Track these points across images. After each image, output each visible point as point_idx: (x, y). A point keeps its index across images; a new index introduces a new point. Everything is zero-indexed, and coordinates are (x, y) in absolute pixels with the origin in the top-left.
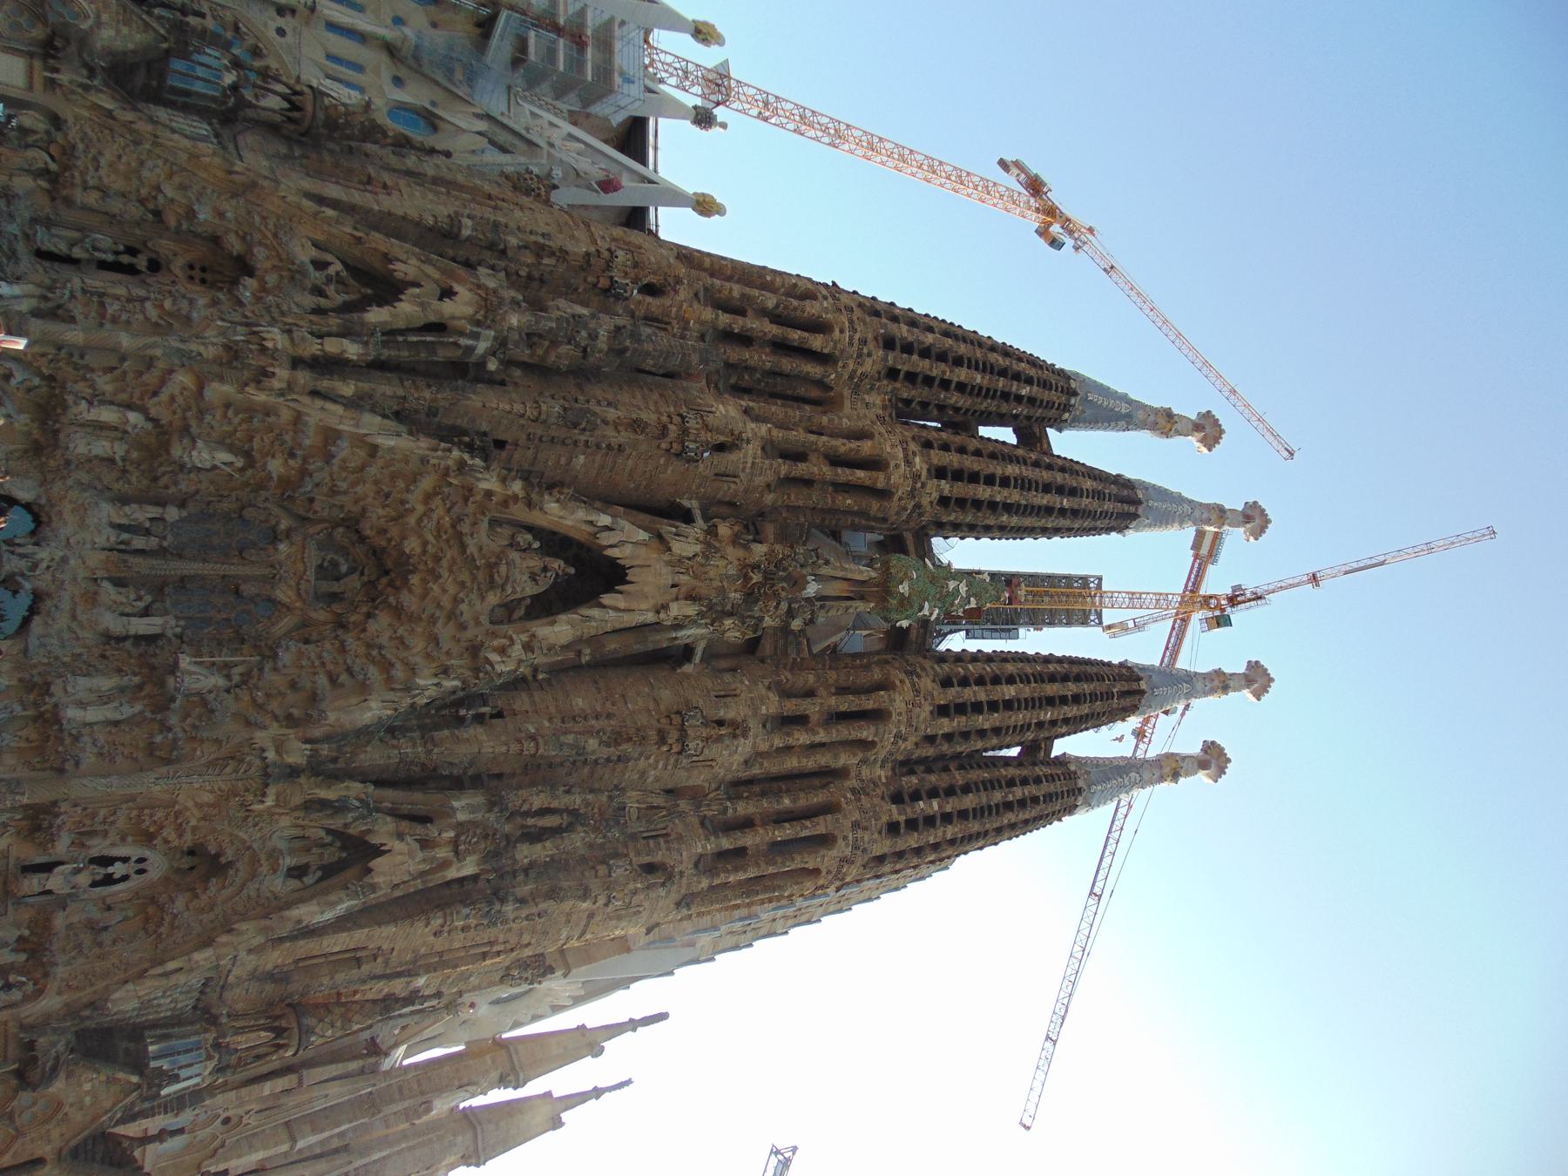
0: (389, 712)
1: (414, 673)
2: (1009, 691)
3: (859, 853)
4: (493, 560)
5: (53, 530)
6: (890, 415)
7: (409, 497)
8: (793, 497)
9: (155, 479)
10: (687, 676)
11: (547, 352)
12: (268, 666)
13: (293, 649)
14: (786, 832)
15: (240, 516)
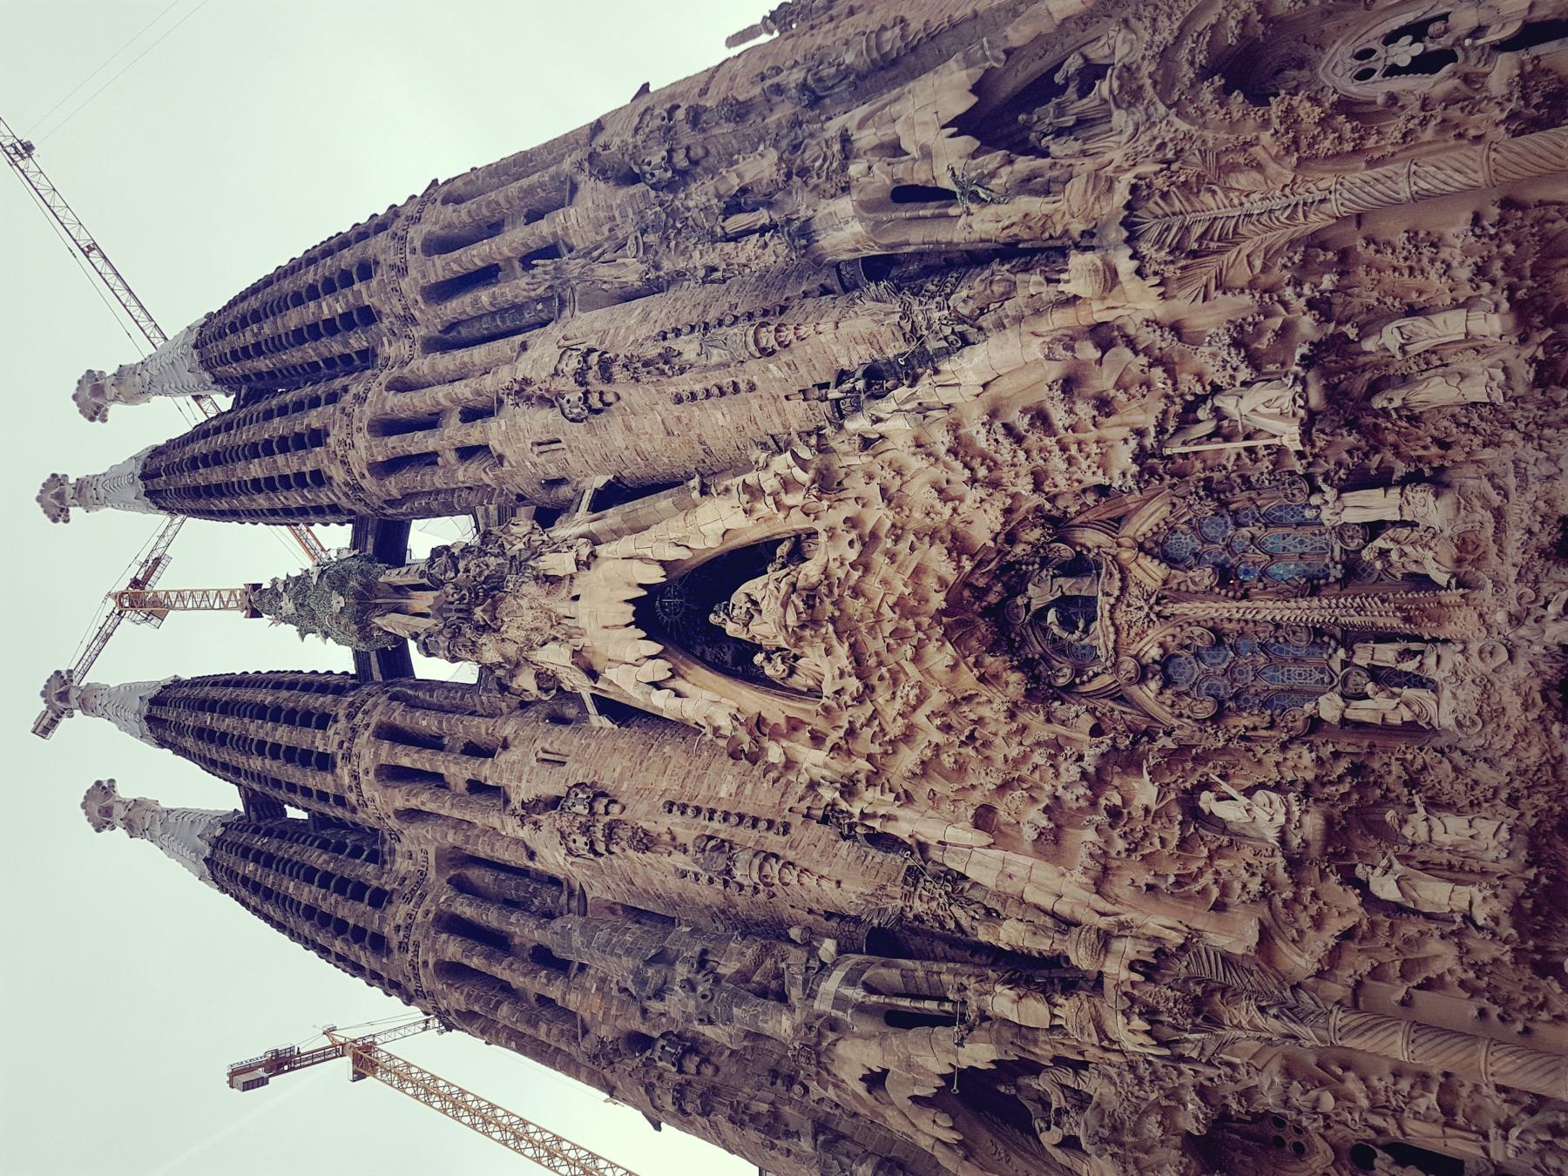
0: (945, 366)
1: (916, 439)
2: (256, 469)
3: (400, 233)
4: (807, 633)
5: (1539, 673)
6: (384, 842)
7: (938, 737)
8: (483, 731)
9: (1356, 770)
10: (599, 470)
11: (758, 963)
12: (1149, 441)
13: (1116, 473)
14: (476, 255)
15: (1220, 703)
